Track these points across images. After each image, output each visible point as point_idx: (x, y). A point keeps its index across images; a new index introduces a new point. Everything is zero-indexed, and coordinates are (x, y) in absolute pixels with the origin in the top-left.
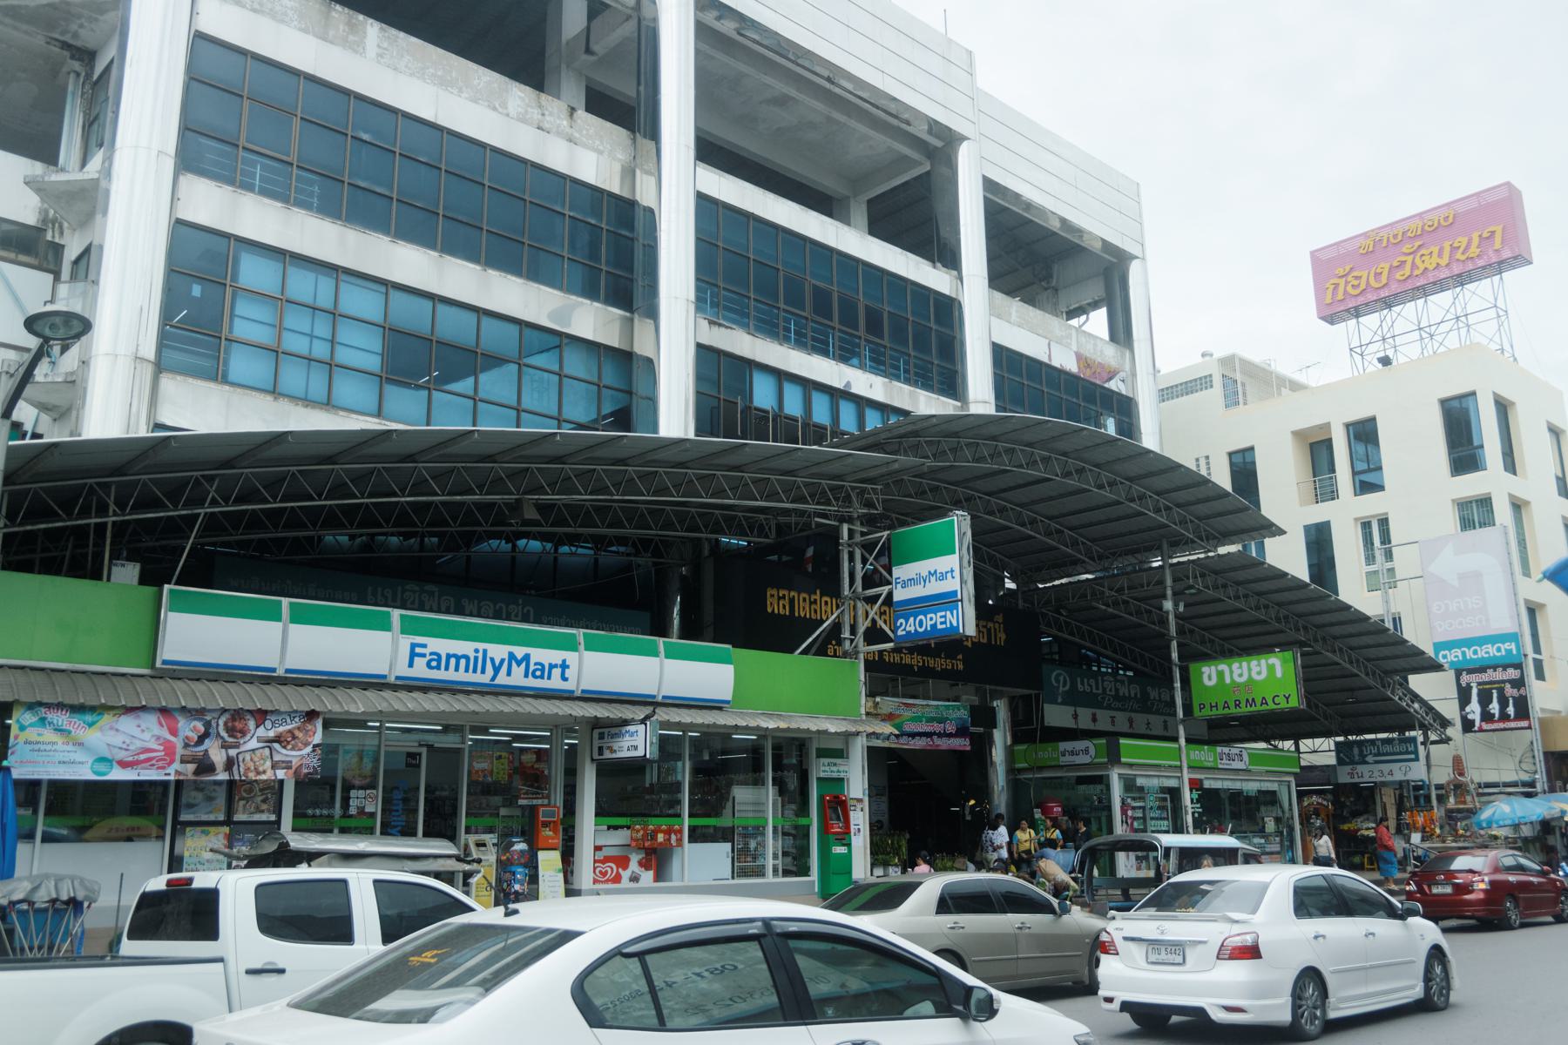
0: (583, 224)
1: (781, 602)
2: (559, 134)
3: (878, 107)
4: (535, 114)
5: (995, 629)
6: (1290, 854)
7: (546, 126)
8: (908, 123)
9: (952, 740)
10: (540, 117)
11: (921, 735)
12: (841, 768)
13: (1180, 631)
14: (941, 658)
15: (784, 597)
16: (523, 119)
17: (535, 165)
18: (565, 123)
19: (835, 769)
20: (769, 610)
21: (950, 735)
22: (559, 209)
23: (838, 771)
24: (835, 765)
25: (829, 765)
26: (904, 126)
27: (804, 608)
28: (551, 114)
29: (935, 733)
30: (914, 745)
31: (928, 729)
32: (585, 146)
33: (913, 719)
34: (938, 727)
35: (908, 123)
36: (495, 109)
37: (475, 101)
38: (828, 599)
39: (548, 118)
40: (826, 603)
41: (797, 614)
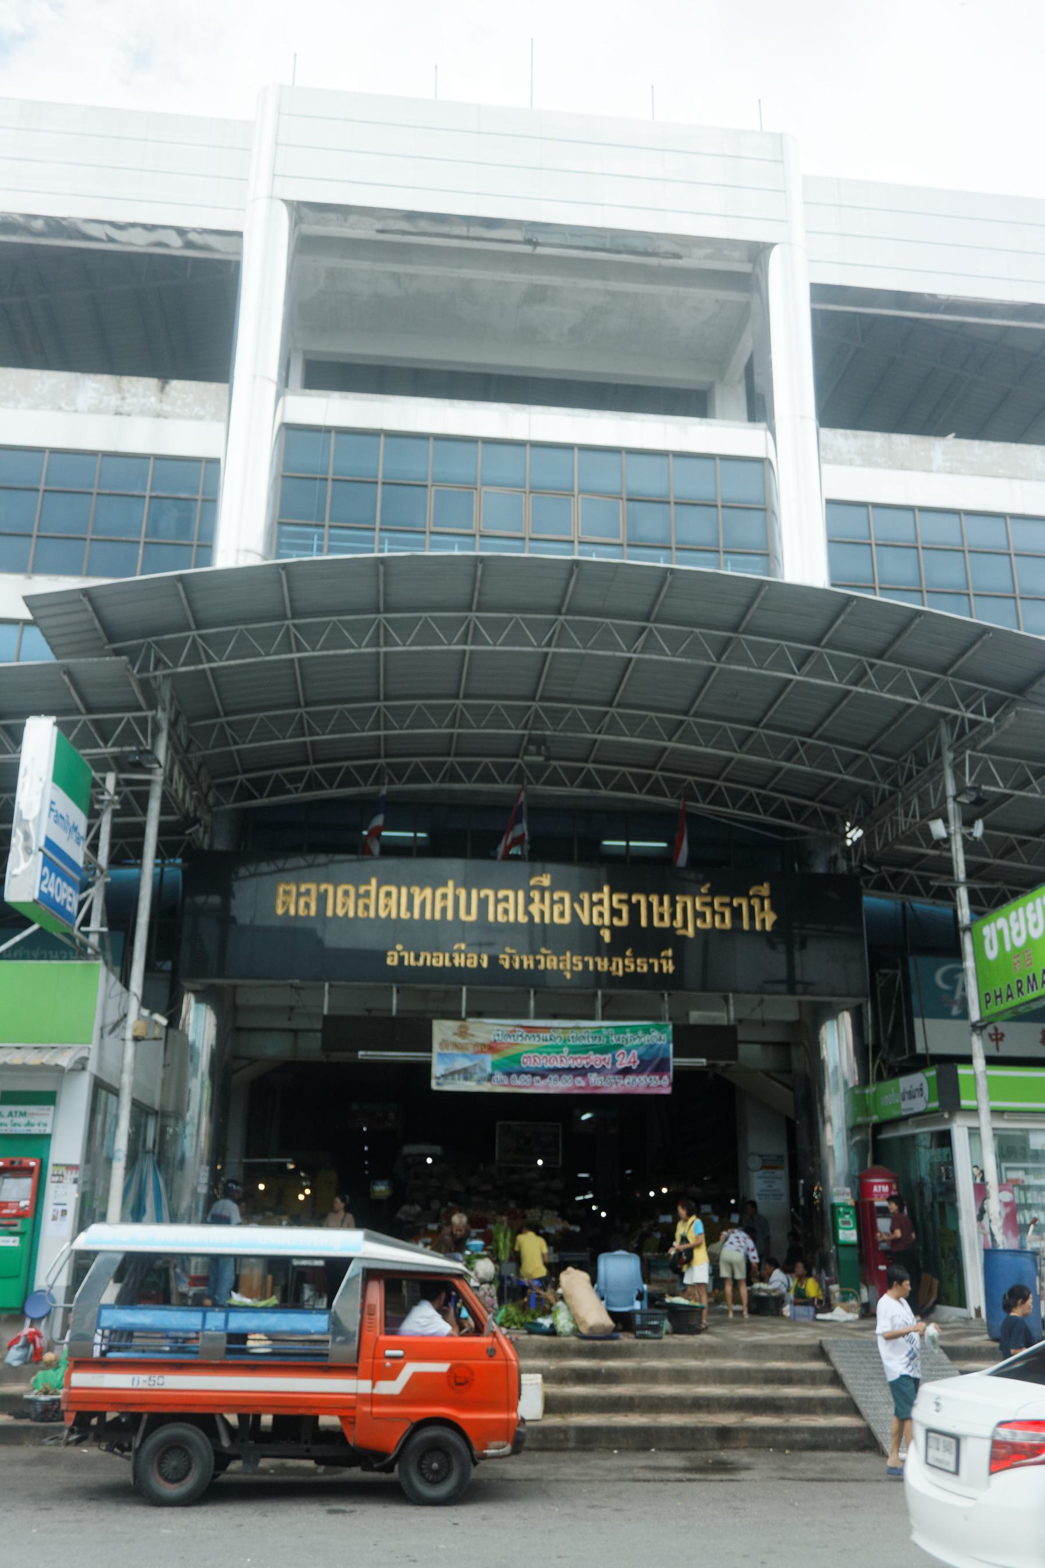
0: (170, 502)
1: (596, 910)
2: (143, 413)
3: (619, 252)
4: (114, 400)
5: (751, 909)
6: (167, 1349)
7: (126, 409)
8: (677, 256)
9: (629, 1079)
10: (119, 402)
11: (569, 1070)
12: (35, 1120)
13: (972, 871)
14: (624, 957)
15: (308, 892)
16: (96, 410)
17: (107, 454)
18: (153, 399)
19: (23, 1120)
20: (280, 911)
21: (626, 1071)
22: (136, 493)
23: (28, 1124)
24: (23, 1114)
25: (10, 1114)
26: (672, 262)
27: (344, 905)
28: (134, 395)
29: (592, 1069)
30: (547, 1086)
31: (574, 1064)
32: (179, 417)
33: (540, 1050)
34: (595, 1059)
35: (677, 256)
36: (60, 409)
37: (36, 407)
38: (394, 890)
39: (128, 401)
40: (388, 894)
41: (644, 923)
